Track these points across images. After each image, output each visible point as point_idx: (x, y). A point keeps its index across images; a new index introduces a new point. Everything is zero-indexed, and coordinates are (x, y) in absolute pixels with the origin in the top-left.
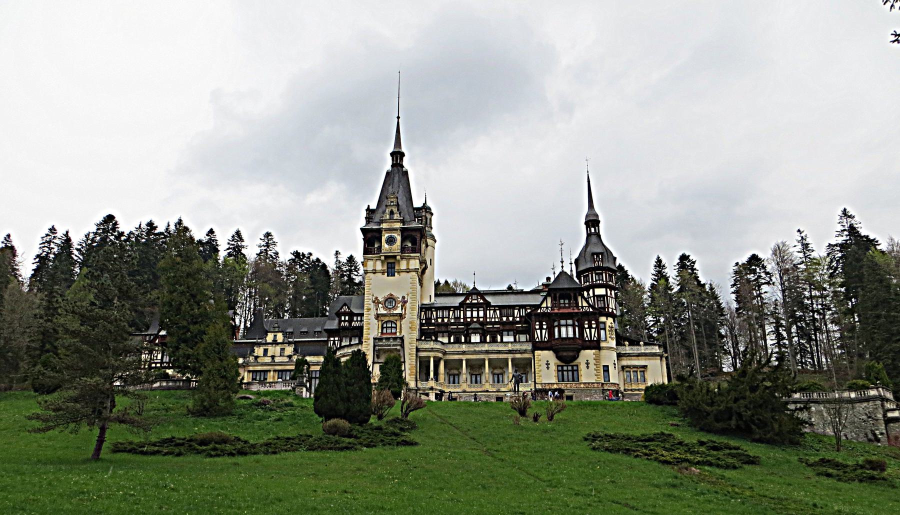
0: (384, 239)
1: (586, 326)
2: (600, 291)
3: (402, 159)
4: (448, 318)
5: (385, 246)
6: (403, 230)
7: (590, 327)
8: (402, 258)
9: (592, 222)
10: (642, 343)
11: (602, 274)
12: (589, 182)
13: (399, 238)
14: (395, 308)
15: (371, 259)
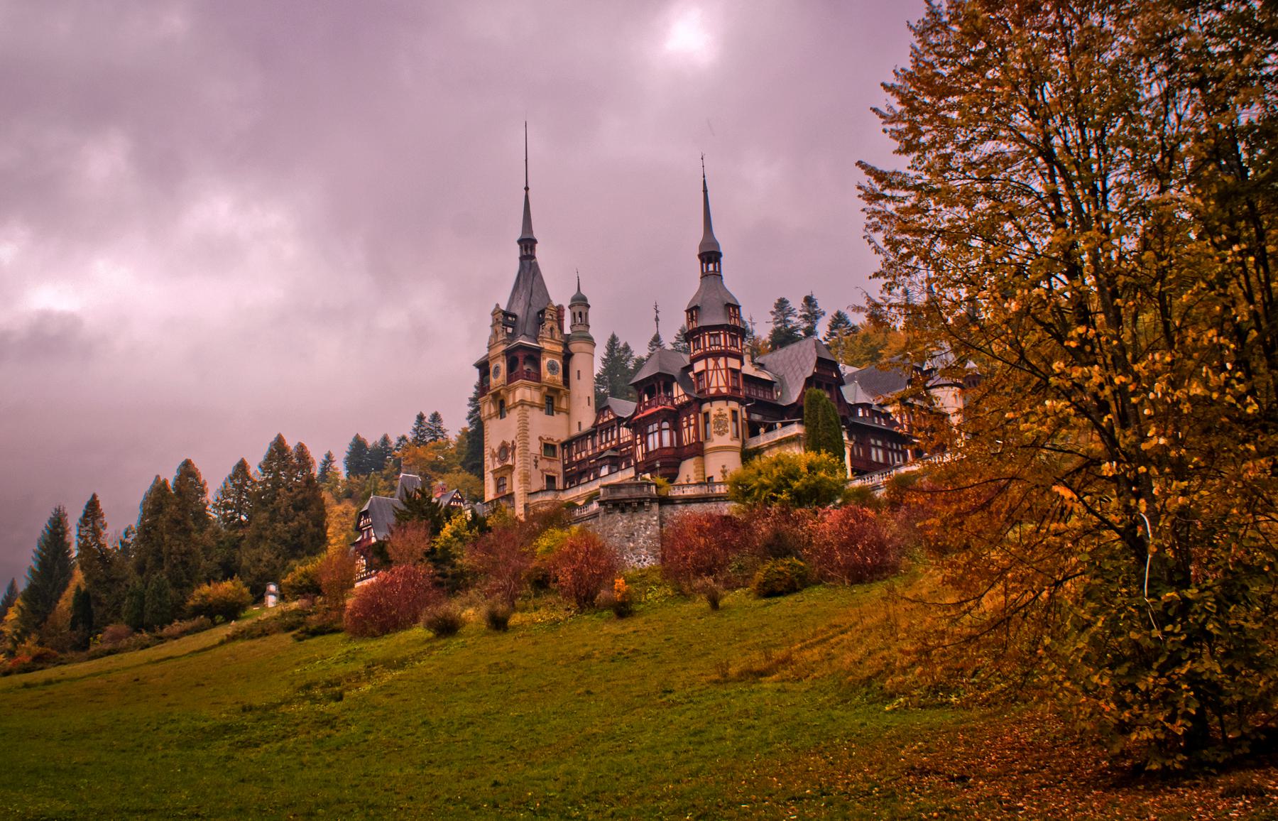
0: (492, 370)
1: (685, 424)
2: (699, 366)
3: (533, 249)
4: (587, 451)
5: (493, 381)
6: (507, 353)
7: (689, 425)
8: (508, 391)
9: (710, 256)
10: (778, 425)
11: (698, 339)
12: (705, 191)
13: (503, 366)
14: (506, 458)
15: (484, 402)
